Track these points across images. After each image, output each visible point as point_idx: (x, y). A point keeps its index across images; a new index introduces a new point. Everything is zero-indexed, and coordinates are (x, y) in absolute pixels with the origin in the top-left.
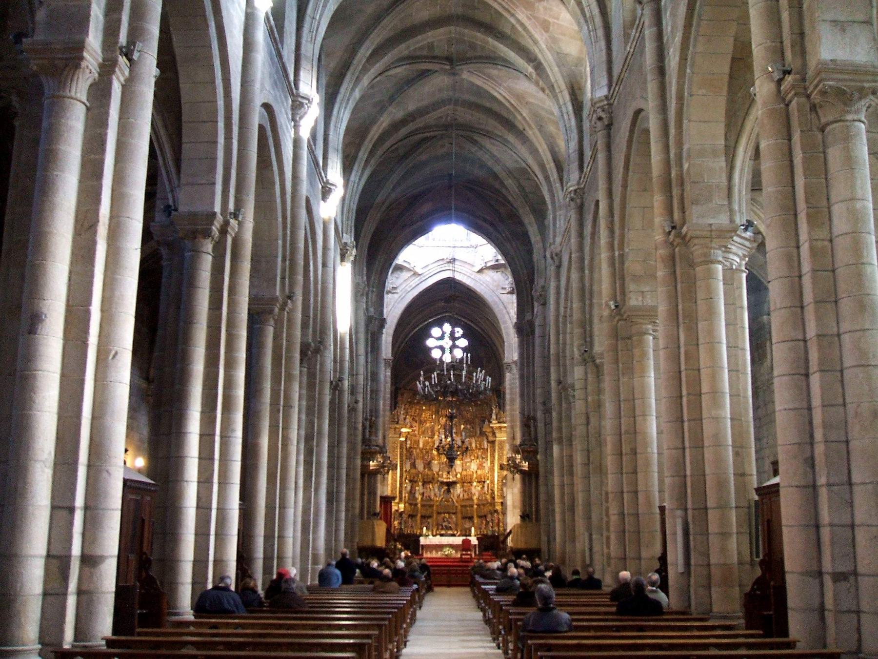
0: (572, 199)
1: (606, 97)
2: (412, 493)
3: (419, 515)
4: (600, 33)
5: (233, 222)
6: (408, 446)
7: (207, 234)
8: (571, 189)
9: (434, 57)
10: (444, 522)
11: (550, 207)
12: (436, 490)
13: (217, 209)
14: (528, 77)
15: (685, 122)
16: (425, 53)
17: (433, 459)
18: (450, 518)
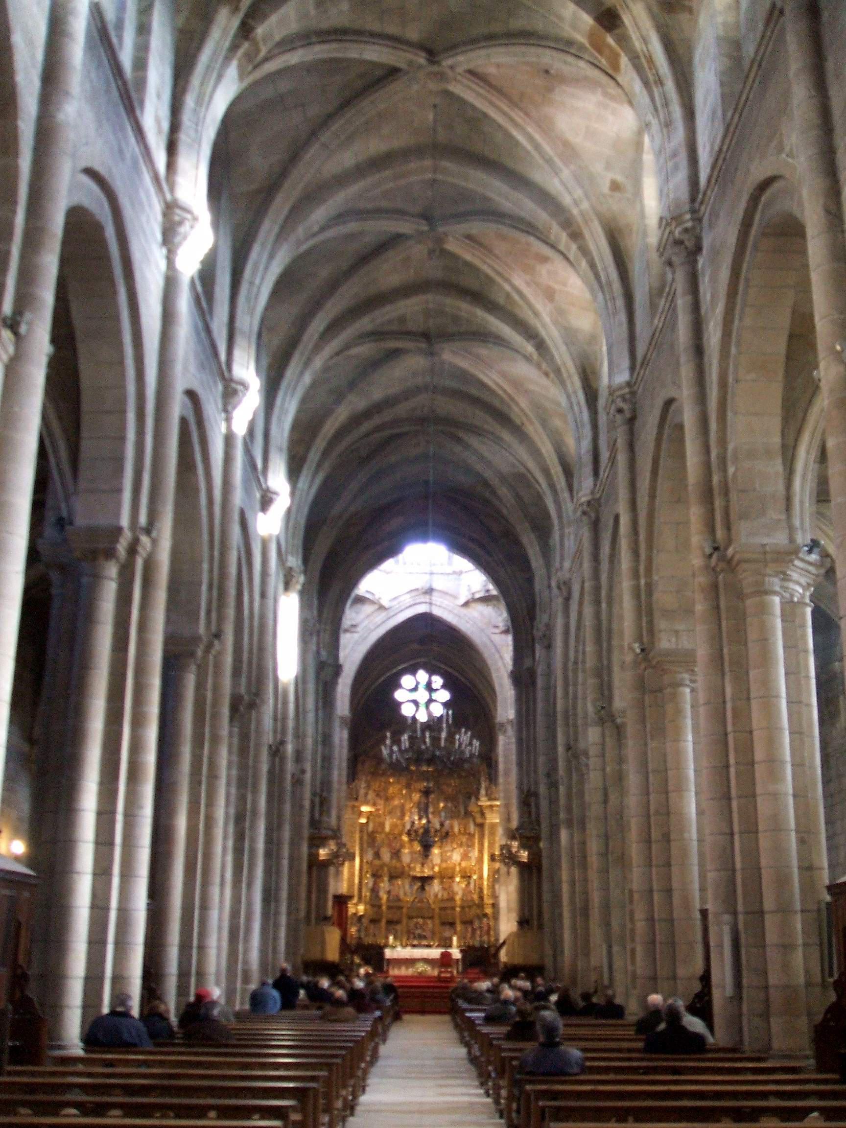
0: (584, 513)
1: (628, 384)
2: (374, 890)
3: (384, 921)
4: (620, 302)
5: (144, 539)
7: (110, 554)
8: (584, 499)
9: (408, 333)
11: (556, 521)
13: (125, 521)
14: (528, 359)
15: (730, 414)
16: (394, 327)
17: (402, 846)
18: (425, 924)
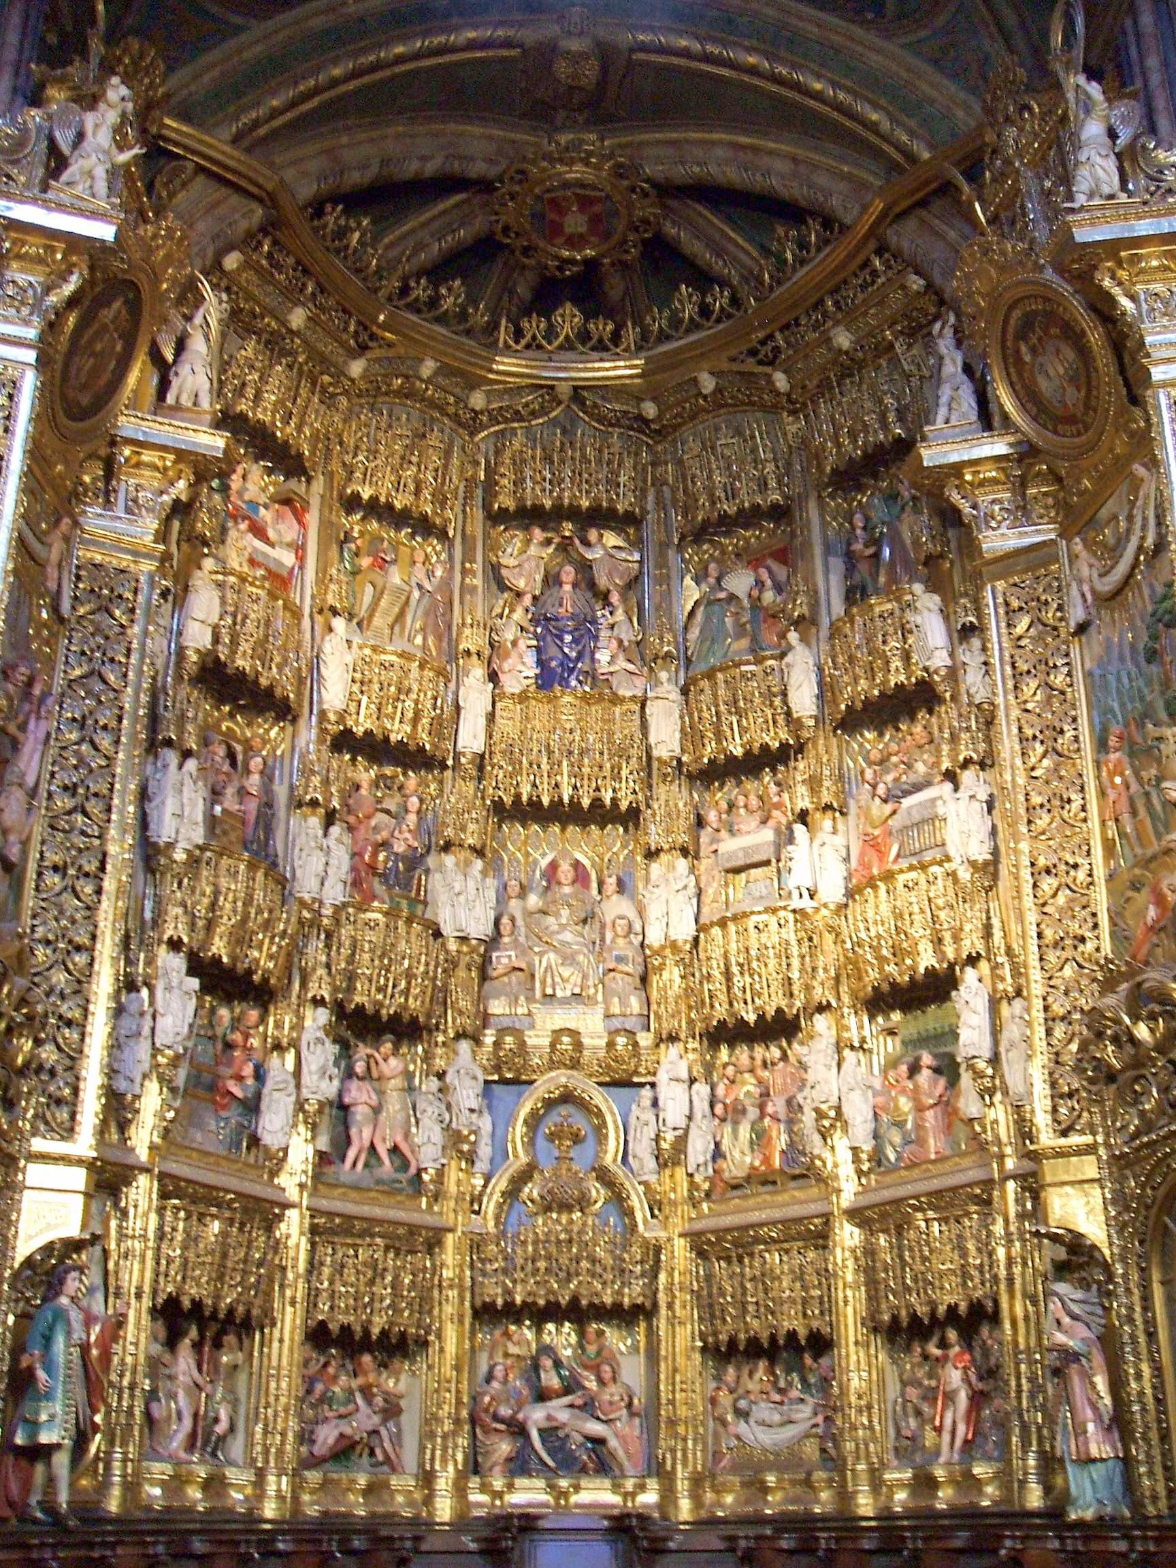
6: (198, 637)
10: (542, 1396)
12: (467, 1094)
18: (601, 1363)
